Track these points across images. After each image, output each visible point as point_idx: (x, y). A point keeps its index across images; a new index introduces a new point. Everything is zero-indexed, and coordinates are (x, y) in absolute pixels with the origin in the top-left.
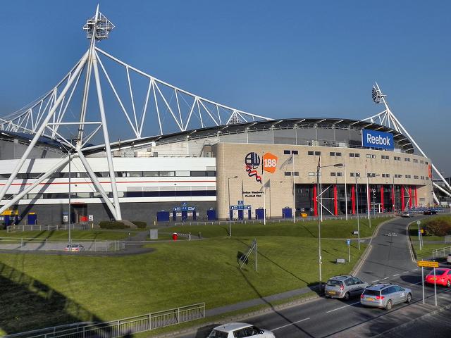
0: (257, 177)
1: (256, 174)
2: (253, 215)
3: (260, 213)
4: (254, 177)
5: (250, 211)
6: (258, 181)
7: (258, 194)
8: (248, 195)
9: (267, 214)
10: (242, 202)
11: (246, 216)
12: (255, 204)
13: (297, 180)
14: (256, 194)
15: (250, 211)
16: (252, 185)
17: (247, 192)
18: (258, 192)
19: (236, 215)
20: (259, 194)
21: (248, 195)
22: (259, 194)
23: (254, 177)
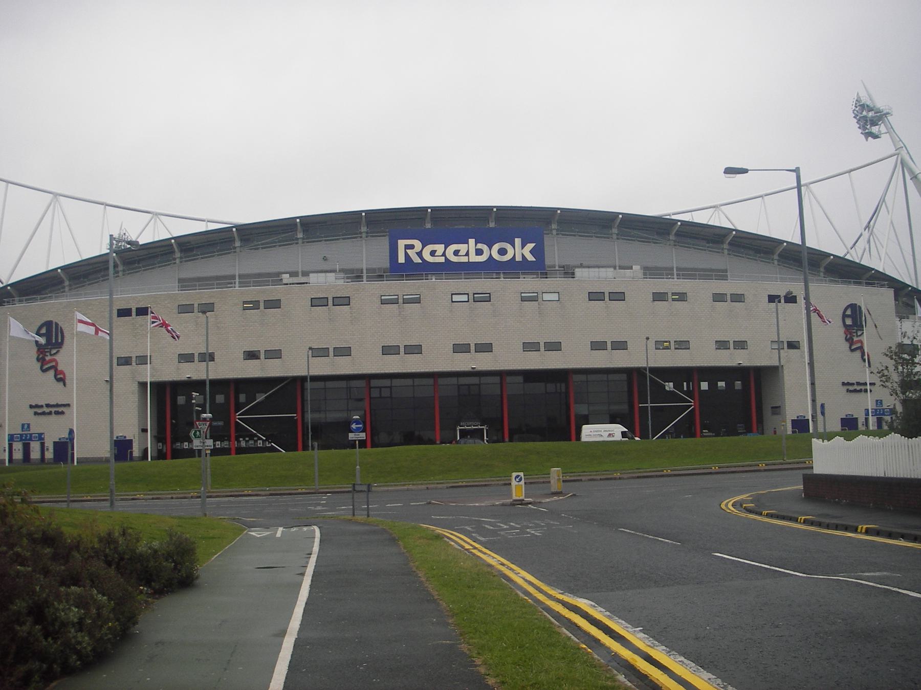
0: (57, 372)
1: (55, 368)
2: (49, 455)
3: (63, 449)
4: (52, 372)
5: (43, 445)
6: (58, 380)
7: (59, 409)
8: (40, 411)
9: (78, 452)
10: (29, 425)
11: (35, 454)
12: (53, 430)
13: (148, 375)
14: (53, 410)
15: (43, 445)
16: (46, 390)
17: (37, 406)
18: (57, 406)
19: (18, 455)
20: (60, 409)
21: (40, 411)
22: (60, 409)
23: (51, 373)
